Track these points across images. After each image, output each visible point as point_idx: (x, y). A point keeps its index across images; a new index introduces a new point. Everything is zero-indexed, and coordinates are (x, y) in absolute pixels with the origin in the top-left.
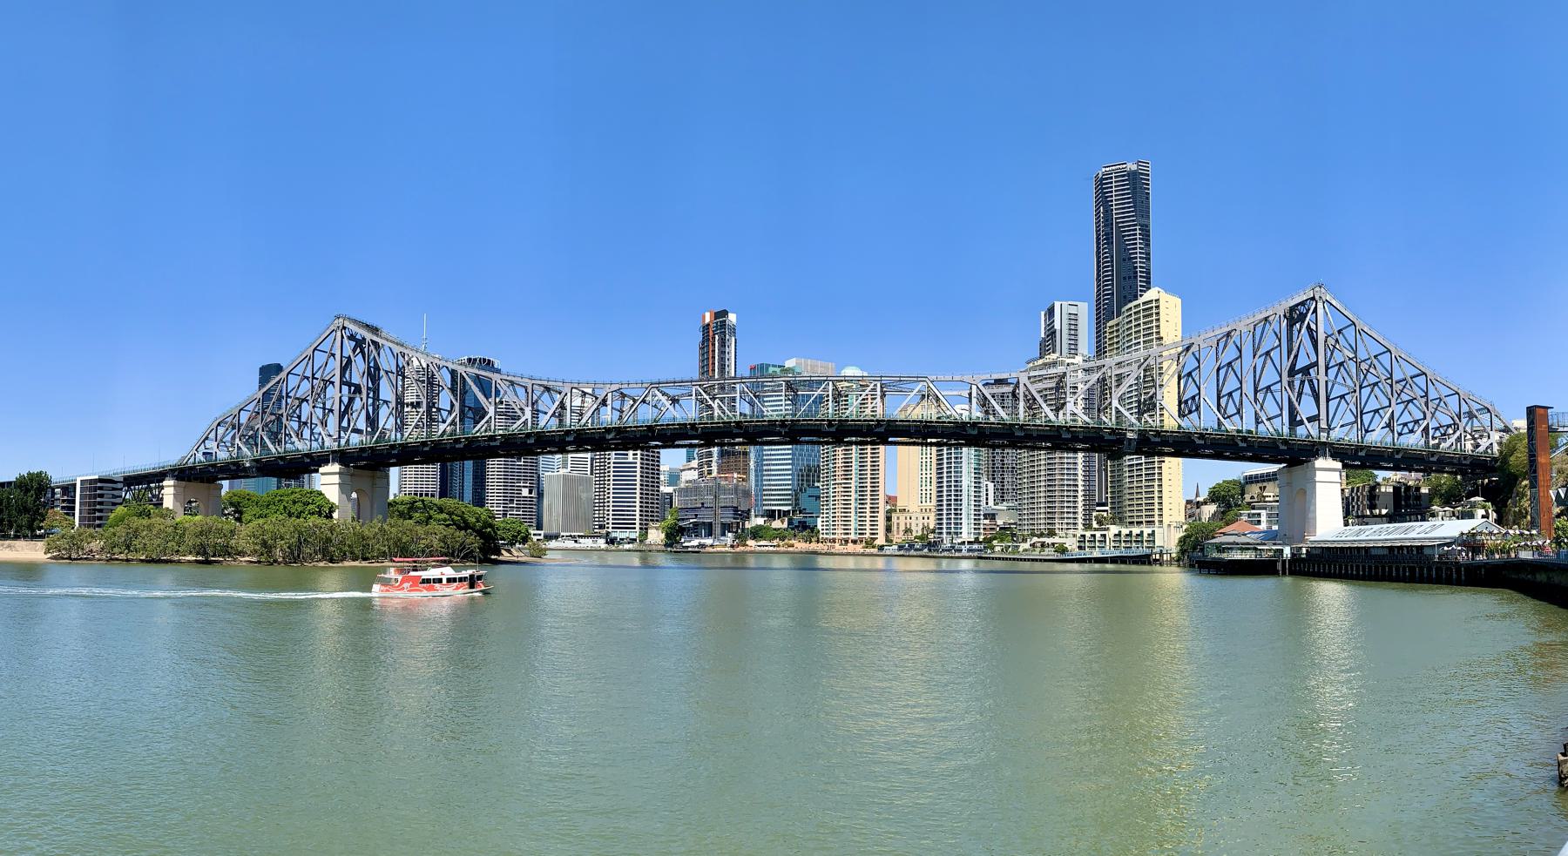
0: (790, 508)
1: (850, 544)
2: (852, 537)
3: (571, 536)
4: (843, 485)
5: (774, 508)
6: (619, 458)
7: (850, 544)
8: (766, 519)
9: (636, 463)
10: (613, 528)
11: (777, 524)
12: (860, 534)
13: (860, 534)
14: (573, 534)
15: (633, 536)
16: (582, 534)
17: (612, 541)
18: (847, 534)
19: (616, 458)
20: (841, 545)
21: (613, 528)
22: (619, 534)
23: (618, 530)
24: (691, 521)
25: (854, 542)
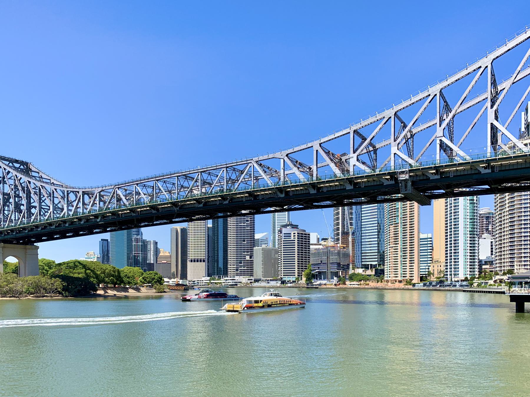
0: (376, 263)
1: (397, 283)
2: (399, 278)
3: (266, 280)
4: (394, 248)
5: (368, 263)
6: (286, 238)
7: (397, 283)
8: (364, 269)
9: (295, 240)
10: (284, 275)
11: (369, 272)
12: (404, 277)
13: (404, 277)
14: (267, 279)
15: (294, 279)
16: (272, 279)
17: (283, 282)
18: (396, 277)
19: (284, 238)
20: (392, 283)
21: (284, 275)
22: (286, 279)
23: (291, 276)
24: (317, 271)
25: (400, 282)
